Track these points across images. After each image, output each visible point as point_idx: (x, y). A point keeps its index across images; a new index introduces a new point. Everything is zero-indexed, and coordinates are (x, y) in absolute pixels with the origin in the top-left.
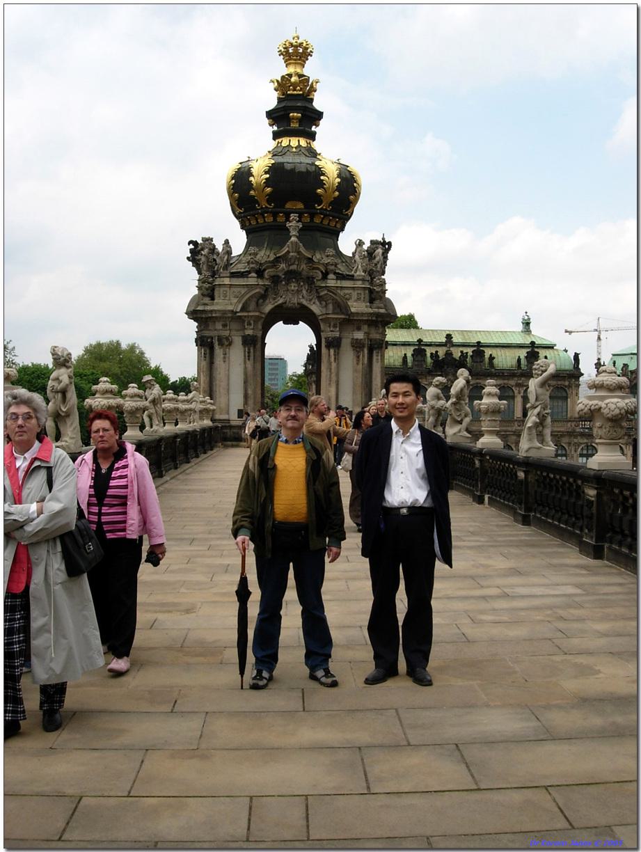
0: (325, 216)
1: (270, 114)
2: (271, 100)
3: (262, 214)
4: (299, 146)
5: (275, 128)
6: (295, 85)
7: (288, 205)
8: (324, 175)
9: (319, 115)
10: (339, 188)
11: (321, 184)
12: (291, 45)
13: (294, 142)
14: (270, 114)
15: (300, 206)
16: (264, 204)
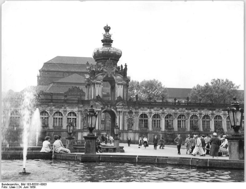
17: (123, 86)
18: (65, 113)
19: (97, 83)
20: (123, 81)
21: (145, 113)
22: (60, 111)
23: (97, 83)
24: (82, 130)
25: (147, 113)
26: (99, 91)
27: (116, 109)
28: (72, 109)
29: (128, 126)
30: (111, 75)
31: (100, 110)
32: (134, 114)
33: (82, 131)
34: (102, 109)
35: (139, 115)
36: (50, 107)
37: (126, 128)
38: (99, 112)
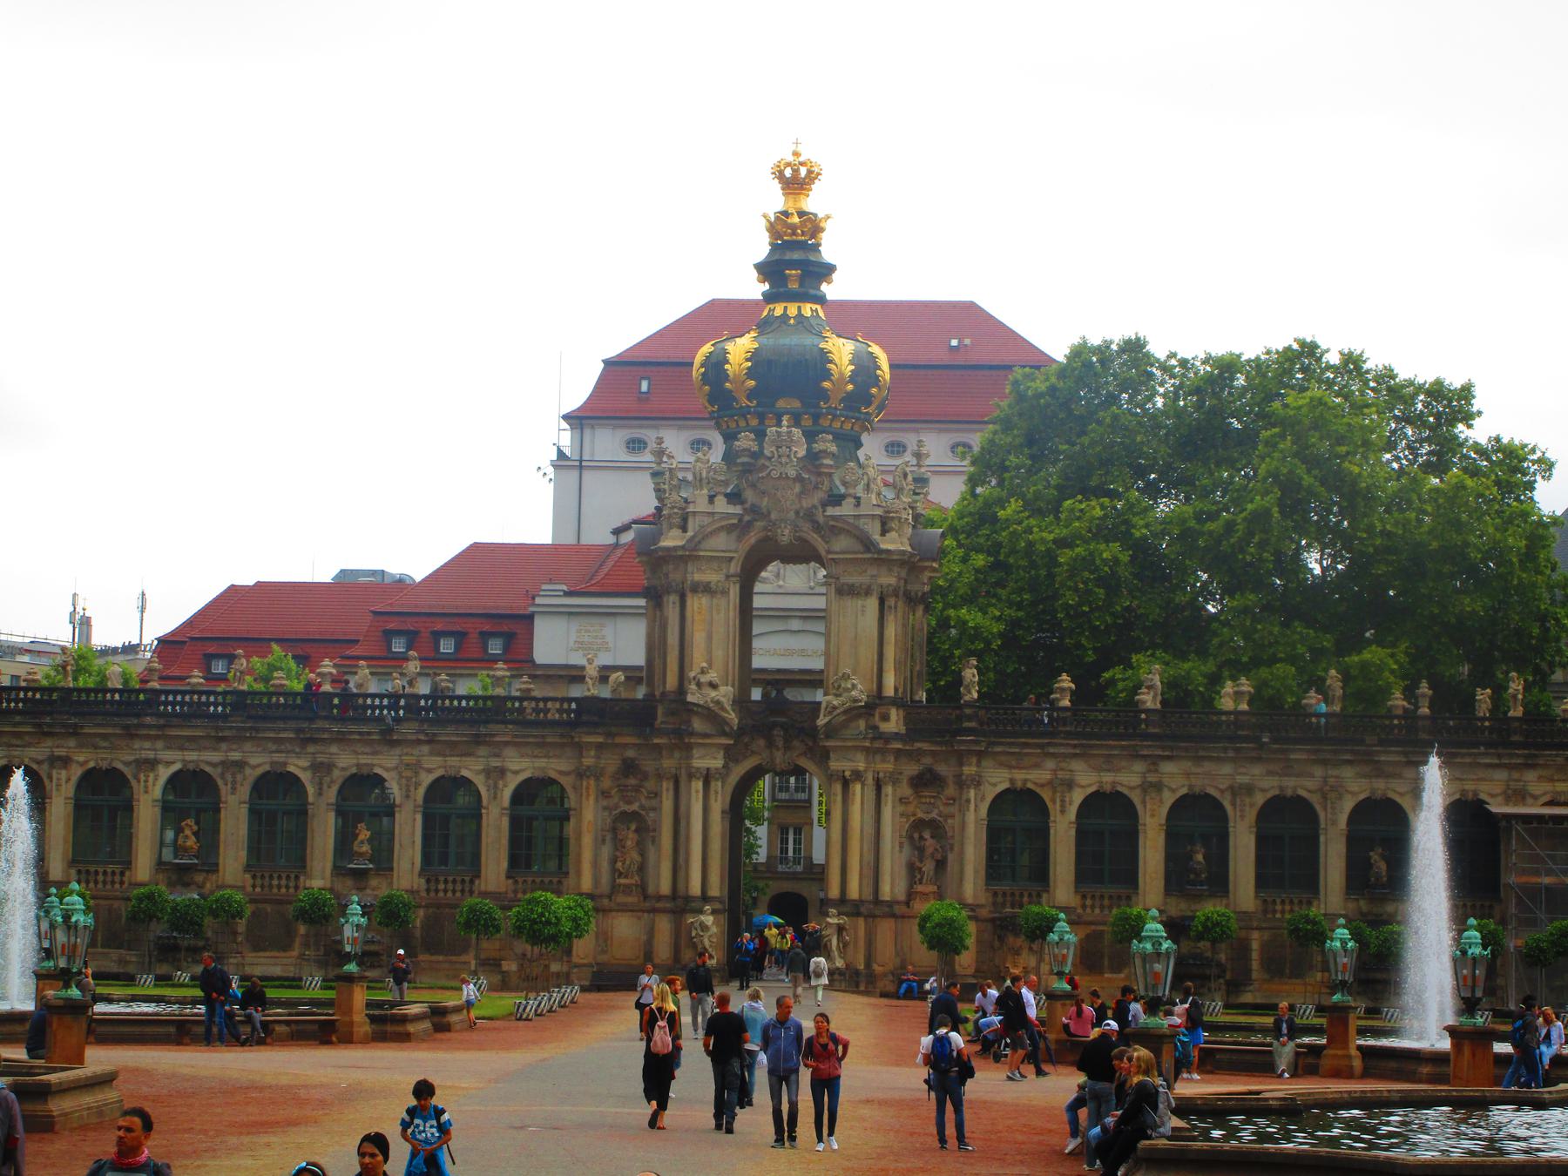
0: (835, 417)
1: (760, 268)
2: (761, 248)
3: (744, 416)
4: (800, 315)
5: (767, 286)
6: (793, 227)
7: (781, 404)
8: (831, 362)
9: (831, 269)
10: (852, 379)
11: (827, 375)
12: (788, 164)
13: (792, 310)
14: (760, 268)
15: (796, 404)
16: (744, 402)
17: (872, 604)
18: (496, 786)
19: (707, 589)
20: (872, 571)
21: (1029, 785)
22: (465, 773)
23: (707, 589)
24: (601, 896)
25: (1042, 786)
26: (710, 638)
27: (823, 757)
28: (541, 762)
29: (913, 870)
30: (796, 528)
31: (717, 763)
32: (951, 790)
33: (606, 901)
34: (732, 756)
35: (983, 798)
36: (398, 751)
37: (892, 886)
38: (707, 784)
